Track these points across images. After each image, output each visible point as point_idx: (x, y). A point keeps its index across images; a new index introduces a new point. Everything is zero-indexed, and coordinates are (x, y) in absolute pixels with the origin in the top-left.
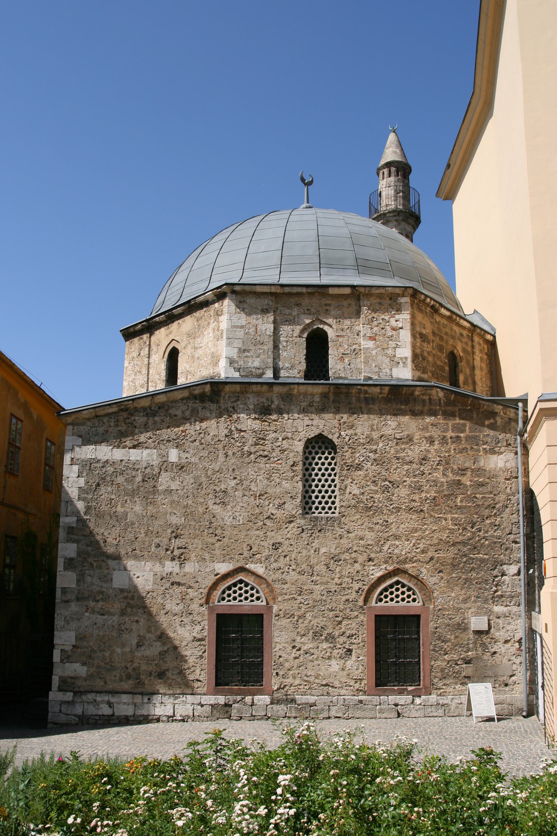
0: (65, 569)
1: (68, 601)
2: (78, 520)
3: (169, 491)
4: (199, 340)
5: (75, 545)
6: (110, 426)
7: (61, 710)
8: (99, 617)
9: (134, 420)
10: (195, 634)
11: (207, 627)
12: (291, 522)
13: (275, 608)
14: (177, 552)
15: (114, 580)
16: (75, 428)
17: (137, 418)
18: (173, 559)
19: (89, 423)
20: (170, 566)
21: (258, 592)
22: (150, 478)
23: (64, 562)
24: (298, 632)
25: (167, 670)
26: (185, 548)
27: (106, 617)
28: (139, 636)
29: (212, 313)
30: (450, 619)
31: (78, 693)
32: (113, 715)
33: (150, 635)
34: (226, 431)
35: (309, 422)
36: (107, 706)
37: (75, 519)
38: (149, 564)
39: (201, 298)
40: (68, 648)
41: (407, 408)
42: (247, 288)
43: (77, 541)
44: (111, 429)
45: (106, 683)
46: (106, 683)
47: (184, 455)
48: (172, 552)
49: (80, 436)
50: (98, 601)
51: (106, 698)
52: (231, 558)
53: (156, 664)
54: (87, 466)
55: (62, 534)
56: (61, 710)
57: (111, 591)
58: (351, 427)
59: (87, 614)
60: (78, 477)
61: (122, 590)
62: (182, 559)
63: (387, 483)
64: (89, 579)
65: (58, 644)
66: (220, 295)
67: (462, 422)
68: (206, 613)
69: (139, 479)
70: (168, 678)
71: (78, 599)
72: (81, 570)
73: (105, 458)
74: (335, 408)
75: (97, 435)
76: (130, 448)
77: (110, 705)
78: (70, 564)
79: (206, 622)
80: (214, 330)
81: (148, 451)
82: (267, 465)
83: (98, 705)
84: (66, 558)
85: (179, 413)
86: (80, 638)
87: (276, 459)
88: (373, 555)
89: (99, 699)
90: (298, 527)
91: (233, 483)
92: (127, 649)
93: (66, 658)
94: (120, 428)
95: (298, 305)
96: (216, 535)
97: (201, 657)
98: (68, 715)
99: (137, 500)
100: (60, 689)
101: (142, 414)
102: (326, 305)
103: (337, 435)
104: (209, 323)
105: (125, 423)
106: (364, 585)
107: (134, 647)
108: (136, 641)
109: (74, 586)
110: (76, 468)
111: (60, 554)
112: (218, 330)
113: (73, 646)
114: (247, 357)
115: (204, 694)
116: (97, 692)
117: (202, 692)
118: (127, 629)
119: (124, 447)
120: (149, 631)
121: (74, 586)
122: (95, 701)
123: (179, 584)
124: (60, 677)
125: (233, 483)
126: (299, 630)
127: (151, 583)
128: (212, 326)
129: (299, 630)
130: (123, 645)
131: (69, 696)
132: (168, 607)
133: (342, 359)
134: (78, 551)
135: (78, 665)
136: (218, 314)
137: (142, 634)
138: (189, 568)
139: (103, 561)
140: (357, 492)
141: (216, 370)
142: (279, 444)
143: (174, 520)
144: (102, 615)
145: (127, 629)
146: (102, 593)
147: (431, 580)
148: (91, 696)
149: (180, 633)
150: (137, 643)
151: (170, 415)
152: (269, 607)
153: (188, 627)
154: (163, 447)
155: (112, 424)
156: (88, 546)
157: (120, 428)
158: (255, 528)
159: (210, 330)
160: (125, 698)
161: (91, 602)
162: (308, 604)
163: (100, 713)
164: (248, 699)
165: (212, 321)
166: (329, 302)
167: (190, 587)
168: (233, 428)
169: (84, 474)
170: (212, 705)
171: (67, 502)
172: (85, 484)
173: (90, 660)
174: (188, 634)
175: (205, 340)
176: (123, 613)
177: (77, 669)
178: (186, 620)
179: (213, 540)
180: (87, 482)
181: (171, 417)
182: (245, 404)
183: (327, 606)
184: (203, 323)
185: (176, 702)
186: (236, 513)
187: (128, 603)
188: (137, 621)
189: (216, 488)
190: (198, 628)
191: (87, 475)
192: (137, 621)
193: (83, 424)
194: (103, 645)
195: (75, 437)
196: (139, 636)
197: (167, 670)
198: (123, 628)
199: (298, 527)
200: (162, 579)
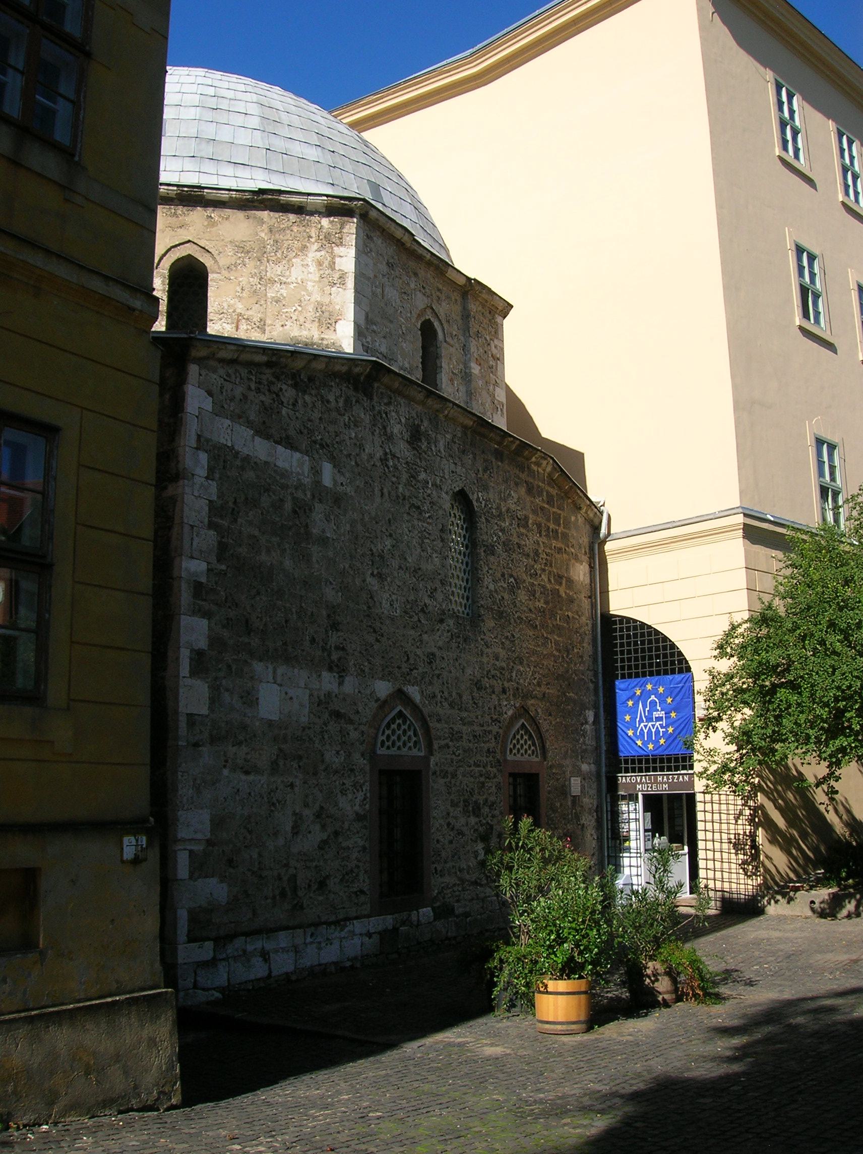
0: (194, 673)
1: (196, 745)
2: (208, 570)
3: (323, 541)
4: (279, 269)
5: (205, 622)
6: (249, 389)
7: (195, 981)
8: (243, 777)
9: (281, 389)
10: (357, 808)
11: (368, 795)
12: (442, 621)
13: (433, 760)
14: (335, 657)
15: (261, 701)
16: (203, 372)
17: (284, 387)
18: (330, 669)
19: (221, 372)
20: (328, 682)
21: (415, 735)
22: (301, 509)
23: (191, 659)
24: (452, 801)
25: (328, 877)
26: (343, 649)
27: (251, 778)
28: (295, 814)
29: (313, 232)
30: (558, 780)
31: (221, 941)
32: (269, 976)
33: (307, 812)
34: (379, 454)
35: (452, 466)
36: (260, 959)
37: (204, 566)
38: (302, 675)
39: (295, 199)
40: (198, 848)
41: (523, 476)
42: (383, 220)
43: (207, 615)
44: (251, 395)
45: (254, 913)
46: (254, 913)
47: (341, 479)
48: (329, 655)
49: (210, 393)
50: (240, 744)
51: (259, 945)
52: (390, 673)
53: (316, 867)
54: (222, 458)
55: (185, 596)
56: (195, 981)
57: (257, 724)
58: (485, 488)
59: (226, 772)
60: (207, 478)
61: (270, 723)
62: (339, 669)
63: (512, 580)
64: (226, 697)
65: (184, 840)
66: (339, 208)
67: (559, 512)
68: (368, 768)
69: (288, 506)
70: (330, 891)
71: (214, 740)
72: (216, 679)
73: (245, 451)
74: (473, 453)
75: (232, 399)
76: (276, 442)
77: (265, 955)
78: (200, 663)
79: (367, 787)
80: (320, 264)
81: (297, 455)
82: (420, 524)
83: (249, 961)
84: (192, 651)
85: (332, 398)
86: (218, 823)
87: (427, 515)
88: (506, 685)
89: (250, 948)
90: (448, 631)
91: (388, 542)
92: (281, 841)
93: (199, 867)
94: (262, 398)
95: (416, 274)
96: (375, 631)
97: (364, 849)
98: (208, 989)
99: (287, 546)
100: (192, 939)
101: (290, 382)
102: (439, 290)
103: (475, 496)
104: (304, 247)
105: (269, 391)
106: (500, 728)
107: (290, 835)
108: (291, 824)
109: (205, 711)
110: (203, 457)
111: (184, 638)
112: (332, 266)
113: (207, 841)
114: (375, 332)
115: (369, 916)
116: (247, 934)
117: (366, 913)
118: (279, 802)
119: (268, 437)
120: (306, 805)
121: (205, 711)
122: (244, 951)
123: (337, 715)
124: (191, 912)
125: (388, 542)
126: (452, 797)
127: (307, 711)
128: (314, 253)
129: (452, 797)
130: (276, 834)
131: (206, 951)
132: (328, 756)
133: (451, 380)
134: (209, 637)
135: (214, 881)
136: (330, 241)
137: (297, 811)
138: (350, 686)
139: (246, 661)
140: (492, 587)
141: (330, 337)
142: (429, 492)
143: (331, 594)
144: (247, 773)
145: (279, 802)
146: (244, 727)
147: (544, 726)
148: (239, 942)
149: (341, 805)
150: (293, 828)
151: (322, 397)
152: (426, 759)
153: (350, 796)
154: (316, 456)
155: (253, 386)
156: (224, 627)
157: (262, 398)
158: (411, 624)
159: (309, 260)
160: (283, 939)
161: (230, 748)
162: (459, 755)
163: (252, 977)
164: (414, 916)
165: (316, 246)
166: (440, 287)
167: (351, 722)
168: (388, 451)
169: (217, 476)
170: (379, 933)
171: (192, 527)
172: (218, 497)
173: (231, 870)
174: (349, 808)
175: (295, 274)
176: (274, 768)
177: (215, 890)
178: (348, 782)
179: (371, 639)
180: (221, 495)
181: (323, 402)
182: (397, 412)
183: (474, 759)
184: (287, 239)
185: (343, 934)
186: (394, 597)
187: (281, 750)
188: (292, 786)
189: (372, 546)
190: (360, 795)
191: (220, 478)
192: (292, 786)
193: (215, 371)
194: (249, 837)
195: (203, 393)
196: (295, 814)
197: (328, 877)
198: (274, 800)
199: (448, 631)
200: (318, 705)
